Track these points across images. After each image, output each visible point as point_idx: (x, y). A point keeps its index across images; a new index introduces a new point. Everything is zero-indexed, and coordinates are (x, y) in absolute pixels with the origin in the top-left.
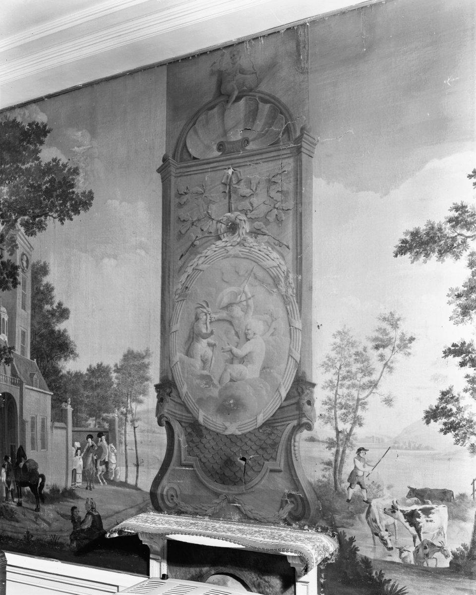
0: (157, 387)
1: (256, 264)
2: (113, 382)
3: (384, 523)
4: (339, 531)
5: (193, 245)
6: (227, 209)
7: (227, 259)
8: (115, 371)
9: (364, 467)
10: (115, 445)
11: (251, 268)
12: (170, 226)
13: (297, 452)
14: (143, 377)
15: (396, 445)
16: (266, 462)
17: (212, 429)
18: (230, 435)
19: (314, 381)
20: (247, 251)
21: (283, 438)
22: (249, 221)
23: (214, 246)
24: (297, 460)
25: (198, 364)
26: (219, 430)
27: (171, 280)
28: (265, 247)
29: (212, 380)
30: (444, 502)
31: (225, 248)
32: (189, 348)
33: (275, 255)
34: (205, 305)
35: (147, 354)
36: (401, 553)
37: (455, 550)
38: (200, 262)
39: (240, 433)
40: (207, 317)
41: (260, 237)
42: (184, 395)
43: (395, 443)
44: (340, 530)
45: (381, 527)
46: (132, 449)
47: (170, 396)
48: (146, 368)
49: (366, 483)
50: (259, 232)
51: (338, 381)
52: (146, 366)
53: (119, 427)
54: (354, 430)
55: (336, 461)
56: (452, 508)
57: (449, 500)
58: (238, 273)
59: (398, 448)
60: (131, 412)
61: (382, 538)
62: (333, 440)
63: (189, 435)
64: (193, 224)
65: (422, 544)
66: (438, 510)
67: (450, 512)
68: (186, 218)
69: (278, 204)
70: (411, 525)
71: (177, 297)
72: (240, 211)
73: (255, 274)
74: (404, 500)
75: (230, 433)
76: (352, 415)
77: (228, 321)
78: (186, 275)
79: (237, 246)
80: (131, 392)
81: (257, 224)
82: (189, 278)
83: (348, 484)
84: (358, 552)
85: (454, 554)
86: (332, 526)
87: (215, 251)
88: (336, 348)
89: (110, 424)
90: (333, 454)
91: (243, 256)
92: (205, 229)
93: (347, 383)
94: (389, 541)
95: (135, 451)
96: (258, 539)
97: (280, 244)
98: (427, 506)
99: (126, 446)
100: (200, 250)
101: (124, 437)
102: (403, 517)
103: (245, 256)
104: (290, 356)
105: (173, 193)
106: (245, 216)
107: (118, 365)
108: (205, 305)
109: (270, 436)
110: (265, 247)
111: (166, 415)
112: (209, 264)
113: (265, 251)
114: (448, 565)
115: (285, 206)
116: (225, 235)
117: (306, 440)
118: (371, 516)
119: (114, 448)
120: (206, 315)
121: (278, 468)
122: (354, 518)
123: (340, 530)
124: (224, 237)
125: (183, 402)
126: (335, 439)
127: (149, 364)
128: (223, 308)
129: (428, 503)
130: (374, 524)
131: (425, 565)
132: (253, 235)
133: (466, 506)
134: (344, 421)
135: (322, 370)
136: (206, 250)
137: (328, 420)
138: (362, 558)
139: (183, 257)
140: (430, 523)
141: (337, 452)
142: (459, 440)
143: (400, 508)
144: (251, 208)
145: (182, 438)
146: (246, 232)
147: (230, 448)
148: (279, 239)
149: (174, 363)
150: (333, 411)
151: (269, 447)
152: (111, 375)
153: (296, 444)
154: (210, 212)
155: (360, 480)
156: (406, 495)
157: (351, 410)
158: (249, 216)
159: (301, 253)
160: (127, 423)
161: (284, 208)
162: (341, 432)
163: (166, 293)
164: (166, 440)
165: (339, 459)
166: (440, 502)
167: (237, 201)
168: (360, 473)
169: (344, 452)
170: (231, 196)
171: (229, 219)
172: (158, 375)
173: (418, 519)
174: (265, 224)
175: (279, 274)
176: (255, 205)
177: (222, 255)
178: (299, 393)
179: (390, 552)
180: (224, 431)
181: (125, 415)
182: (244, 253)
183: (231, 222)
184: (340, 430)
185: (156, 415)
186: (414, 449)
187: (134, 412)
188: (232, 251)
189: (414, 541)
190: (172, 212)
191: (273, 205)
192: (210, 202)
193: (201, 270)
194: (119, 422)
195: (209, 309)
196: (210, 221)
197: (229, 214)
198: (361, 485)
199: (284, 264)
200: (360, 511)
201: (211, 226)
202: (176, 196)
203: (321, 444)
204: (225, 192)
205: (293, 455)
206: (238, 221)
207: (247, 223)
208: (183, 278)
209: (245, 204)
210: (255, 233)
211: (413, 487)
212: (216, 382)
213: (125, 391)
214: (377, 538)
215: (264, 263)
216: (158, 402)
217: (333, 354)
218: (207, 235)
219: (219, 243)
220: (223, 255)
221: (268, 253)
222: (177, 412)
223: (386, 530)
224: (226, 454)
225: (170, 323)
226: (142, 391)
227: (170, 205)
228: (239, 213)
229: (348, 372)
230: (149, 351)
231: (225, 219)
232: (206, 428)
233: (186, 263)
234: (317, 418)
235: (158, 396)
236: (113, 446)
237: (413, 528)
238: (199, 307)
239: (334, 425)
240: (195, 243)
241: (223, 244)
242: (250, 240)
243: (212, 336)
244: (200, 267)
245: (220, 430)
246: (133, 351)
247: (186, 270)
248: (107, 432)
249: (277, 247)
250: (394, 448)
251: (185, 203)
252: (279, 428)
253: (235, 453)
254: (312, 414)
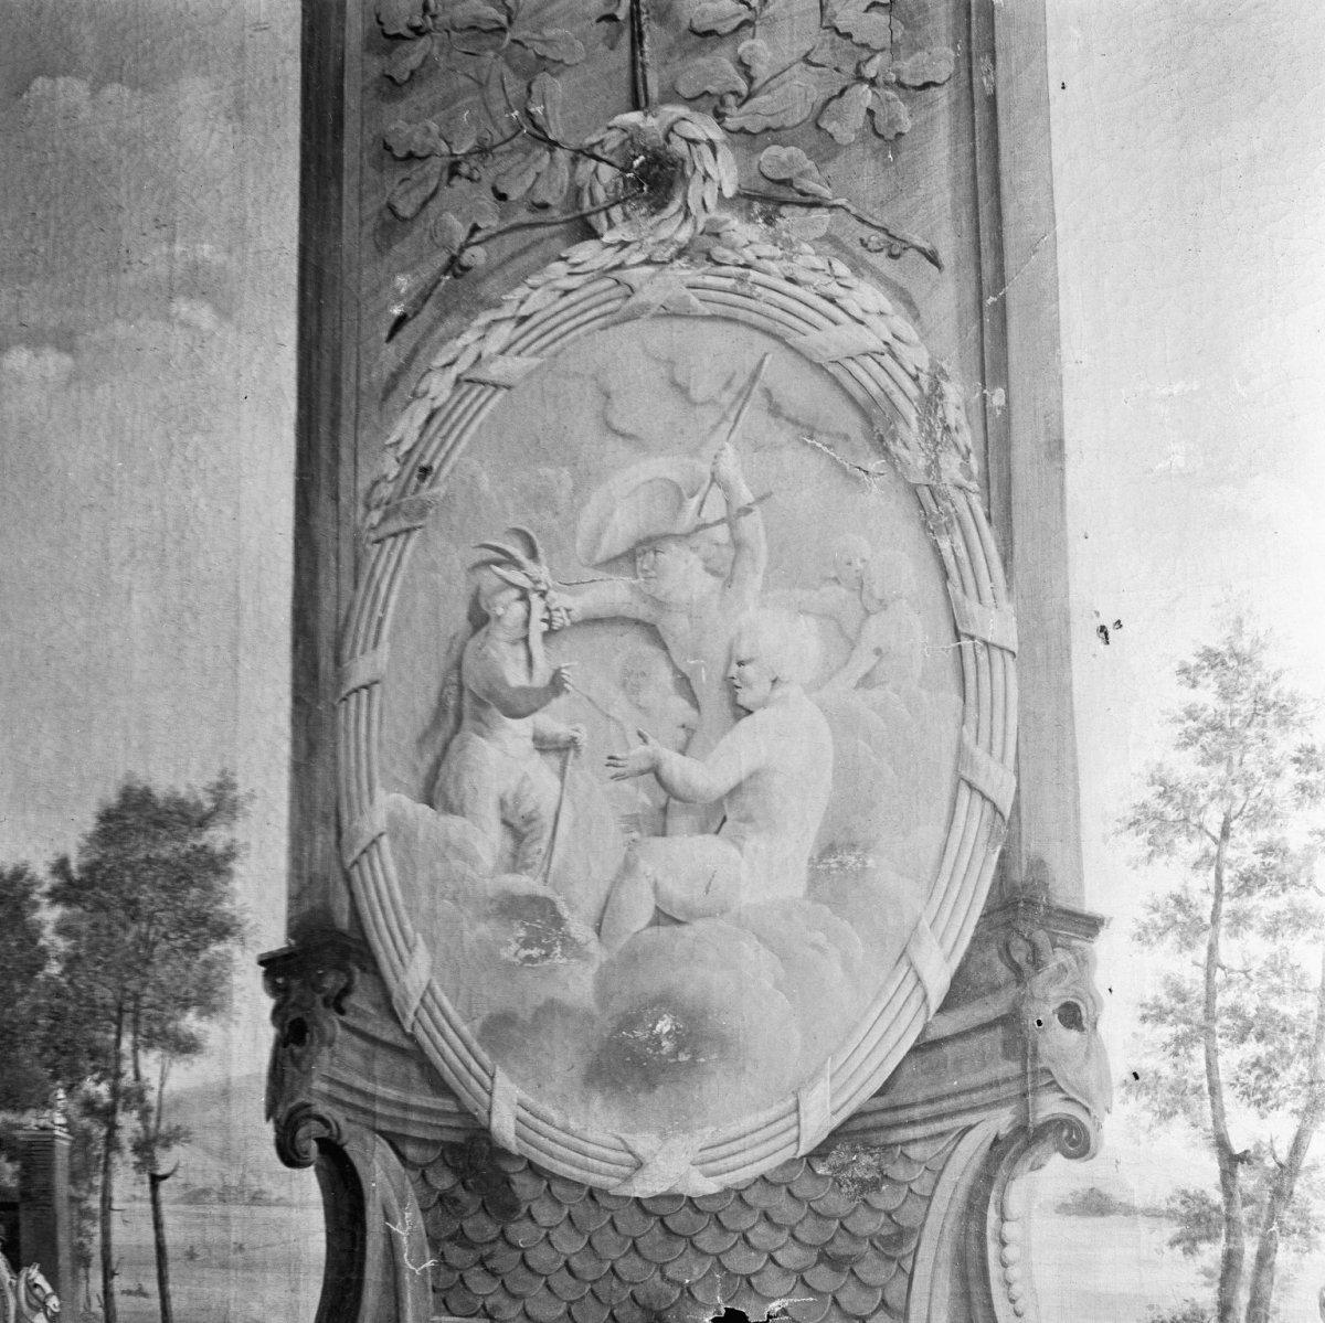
0: (275, 967)
1: (774, 343)
2: (43, 951)
5: (455, 267)
6: (625, 94)
7: (628, 325)
8: (56, 896)
10: (52, 1275)
11: (751, 365)
12: (340, 185)
13: (1014, 1272)
14: (203, 920)
17: (562, 1168)
18: (656, 1198)
19: (1092, 905)
20: (728, 283)
21: (939, 1205)
22: (733, 146)
23: (560, 268)
24: (1018, 1315)
25: (489, 842)
26: (598, 1172)
27: (345, 439)
28: (819, 263)
29: (558, 921)
31: (616, 274)
32: (438, 764)
33: (867, 296)
34: (519, 553)
35: (224, 802)
38: (492, 346)
39: (711, 1186)
40: (529, 612)
41: (791, 217)
42: (415, 1003)
46: (141, 1293)
47: (341, 1011)
48: (218, 872)
50: (784, 193)
51: (1218, 895)
52: (216, 865)
53: (74, 1178)
58: (682, 390)
60: (134, 1098)
62: (1204, 1202)
63: (440, 1206)
64: (453, 170)
68: (418, 142)
69: (878, 58)
71: (376, 517)
72: (689, 101)
73: (768, 393)
75: (660, 1188)
76: (1300, 1067)
77: (637, 622)
78: (420, 412)
79: (678, 263)
80: (137, 997)
81: (774, 157)
82: (435, 423)
87: (567, 292)
88: (1201, 732)
89: (24, 1167)
90: (1208, 1273)
91: (706, 309)
92: (515, 193)
93: (1263, 904)
95: (156, 1302)
97: (895, 247)
99: (108, 1274)
100: (489, 288)
101: (97, 1229)
103: (720, 310)
104: (964, 782)
105: (355, 30)
106: (714, 122)
107: (73, 866)
108: (519, 553)
109: (872, 1197)
110: (819, 263)
111: (321, 1108)
112: (536, 354)
113: (817, 279)
115: (910, 68)
116: (616, 212)
117: (1063, 1209)
119: (48, 1289)
120: (524, 597)
124: (611, 225)
125: (412, 1037)
126: (1217, 1198)
127: (230, 854)
128: (611, 563)
132: (757, 206)
134: (1261, 1100)
135: (1135, 844)
136: (520, 292)
137: (1176, 1100)
139: (407, 329)
141: (1230, 1261)
144: (743, 87)
145: (409, 1225)
146: (721, 196)
147: (661, 1268)
148: (884, 219)
149: (363, 842)
150: (1199, 1052)
151: (870, 1254)
152: (37, 916)
153: (1010, 1230)
154: (537, 109)
157: (1291, 1046)
158: (731, 123)
159: (1000, 280)
160: (116, 1159)
161: (907, 80)
162: (1243, 1158)
163: (324, 506)
164: (323, 1236)
167: (670, 54)
169: (1264, 1258)
170: (641, 35)
171: (632, 137)
172: (281, 908)
174: (811, 153)
175: (892, 387)
176: (761, 71)
177: (603, 309)
178: (1016, 969)
180: (627, 1179)
181: (107, 1115)
182: (713, 294)
183: (644, 150)
184: (1238, 1150)
185: (270, 1112)
187: (151, 1097)
188: (654, 287)
190: (351, 124)
191: (849, 69)
192: (539, 65)
193: (496, 386)
194: (72, 1152)
195: (542, 571)
196: (538, 152)
197: (634, 117)
199: (915, 338)
201: (549, 177)
202: (369, 46)
203: (1143, 1224)
204: (611, 18)
205: (996, 1289)
206: (679, 147)
207: (723, 150)
208: (406, 427)
209: (718, 69)
210: (765, 199)
212: (579, 928)
213: (105, 994)
215: (812, 340)
216: (281, 1043)
217: (1185, 767)
218: (524, 216)
219: (585, 252)
220: (610, 306)
221: (835, 290)
222: (381, 1090)
224: (641, 1298)
225: (338, 647)
226: (194, 994)
227: (340, 91)
228: (682, 111)
229: (1268, 850)
230: (233, 786)
231: (614, 139)
232: (533, 1169)
233: (424, 351)
234: (1118, 1094)
235: (277, 1014)
236: (40, 1280)
238: (487, 564)
239: (1210, 1125)
240: (465, 259)
241: (609, 258)
242: (743, 232)
243: (558, 703)
244: (494, 371)
245: (610, 1175)
246: (147, 794)
247: (423, 387)
248: (13, 1207)
249: (880, 261)
251: (412, 73)
252: (915, 1152)
253: (688, 1291)
254: (1090, 1074)
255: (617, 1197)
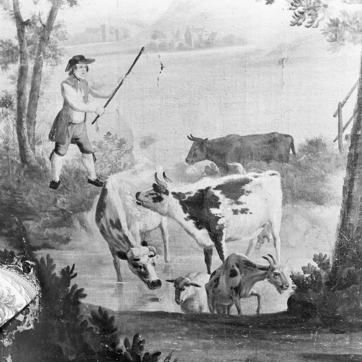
3: (138, 227)
4: (39, 258)
9: (85, 99)
15: (157, 42)
30: (272, 163)
36: (179, 290)
37: (298, 270)
43: (154, 37)
44: (41, 254)
45: (131, 239)
49: (91, 140)
54: (59, 17)
55: (20, 93)
56: (292, 175)
57: (283, 159)
59: (163, 48)
61: (135, 263)
62: (10, 45)
65: (226, 264)
66: (260, 185)
67: (286, 187)
70: (199, 225)
74: (181, 168)
83: (52, 145)
84: (82, 301)
85: (297, 280)
86: (21, 247)
90: (12, 78)
94: (150, 268)
98: (235, 177)
102: (180, 208)
114: (284, 307)
118: (108, 214)
122: (70, 225)
123: (41, 254)
126: (16, 43)
129: (235, 171)
130: (115, 232)
131: (234, 311)
133: (322, 167)
138: (93, 313)
140: (242, 216)
141: (22, 71)
142: (302, 13)
143: (172, 187)
155: (78, 132)
156: (184, 157)
162: (27, 23)
165: (28, 88)
166: (264, 164)
168: (77, 117)
169: (37, 70)
173: (214, 211)
179: (156, 292)
184: (25, 20)
186: (198, 47)
189: (208, 261)
198: (80, 145)
200: (84, 206)
211: (200, 135)
214: (123, 263)
223: (144, 244)
237: (204, 231)
239: (12, 9)
250: (153, 48)
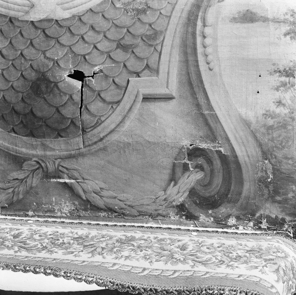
13: (209, 50)
16: (133, 80)
18: (41, 21)
21: (174, 20)
24: (210, 70)
26: (14, 10)
39: (66, 15)
75: (42, 17)
96: (134, 263)
109: (142, 17)
117: (234, 20)
121: (162, 91)
147: (44, 52)
151: (141, 44)
153: (208, 31)
180: (27, 13)
203: (272, 26)
205: (201, 59)
224: (35, 67)
245: (19, 11)
253: (56, 63)
255: (22, 21)
